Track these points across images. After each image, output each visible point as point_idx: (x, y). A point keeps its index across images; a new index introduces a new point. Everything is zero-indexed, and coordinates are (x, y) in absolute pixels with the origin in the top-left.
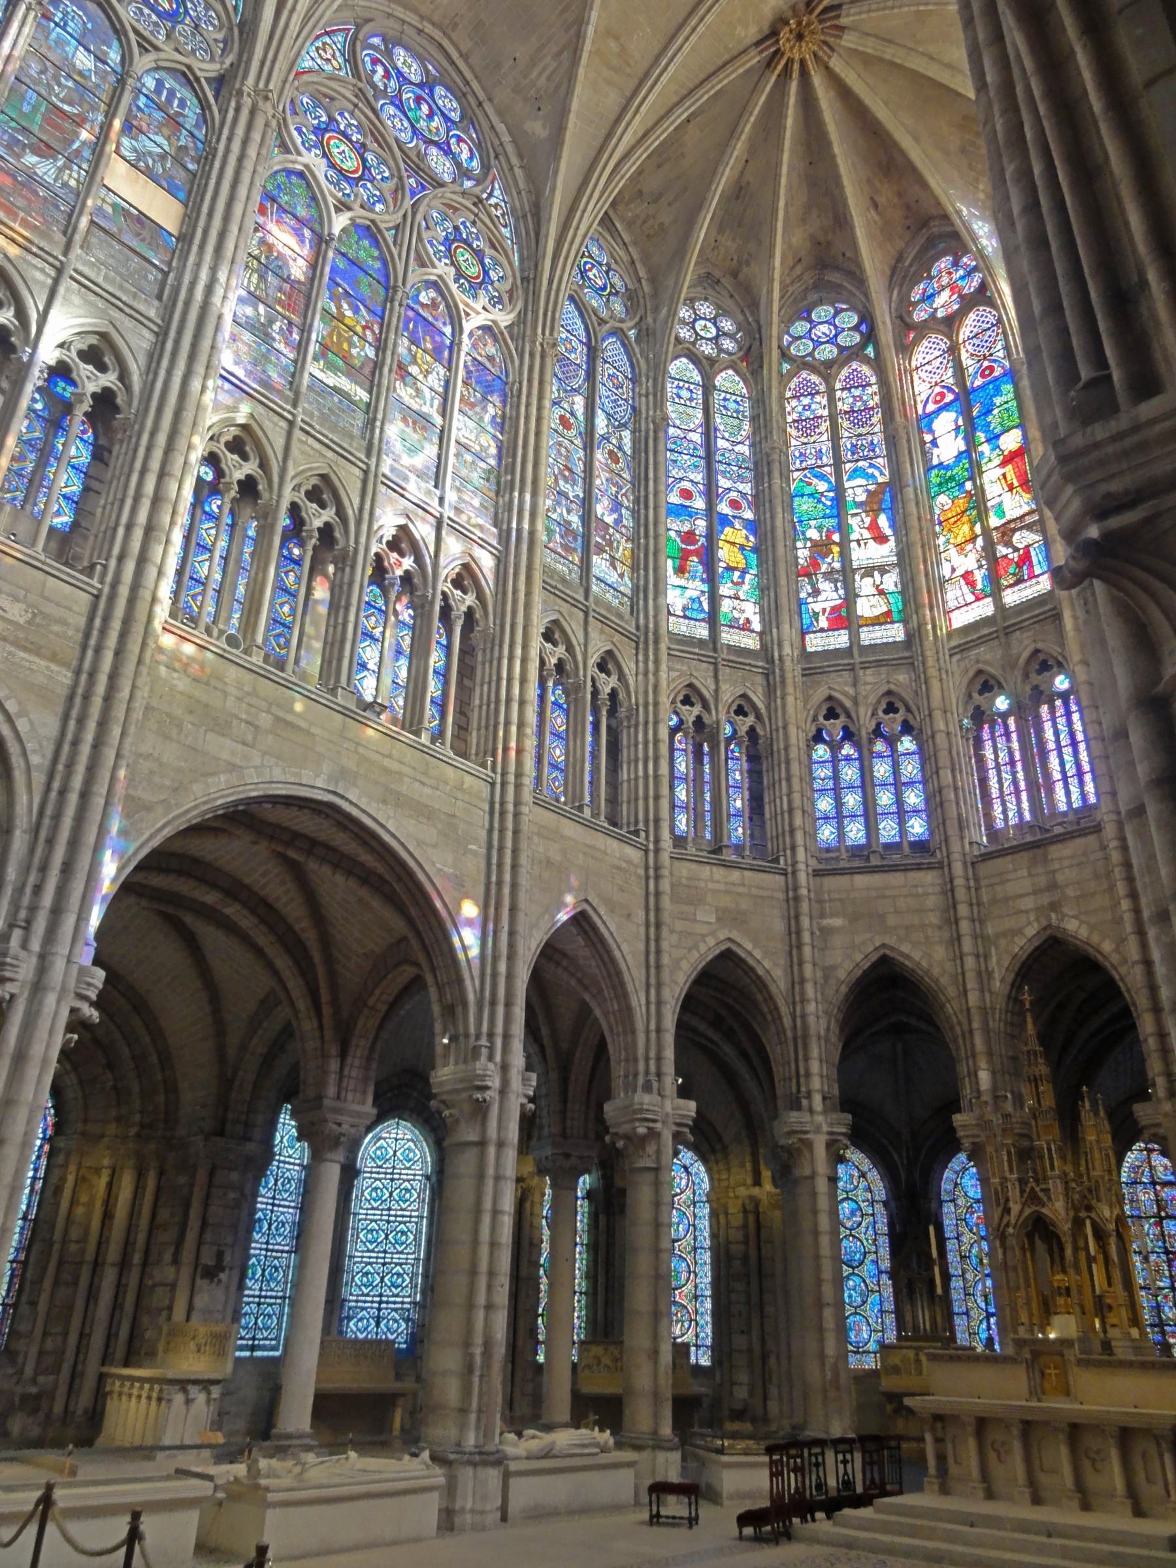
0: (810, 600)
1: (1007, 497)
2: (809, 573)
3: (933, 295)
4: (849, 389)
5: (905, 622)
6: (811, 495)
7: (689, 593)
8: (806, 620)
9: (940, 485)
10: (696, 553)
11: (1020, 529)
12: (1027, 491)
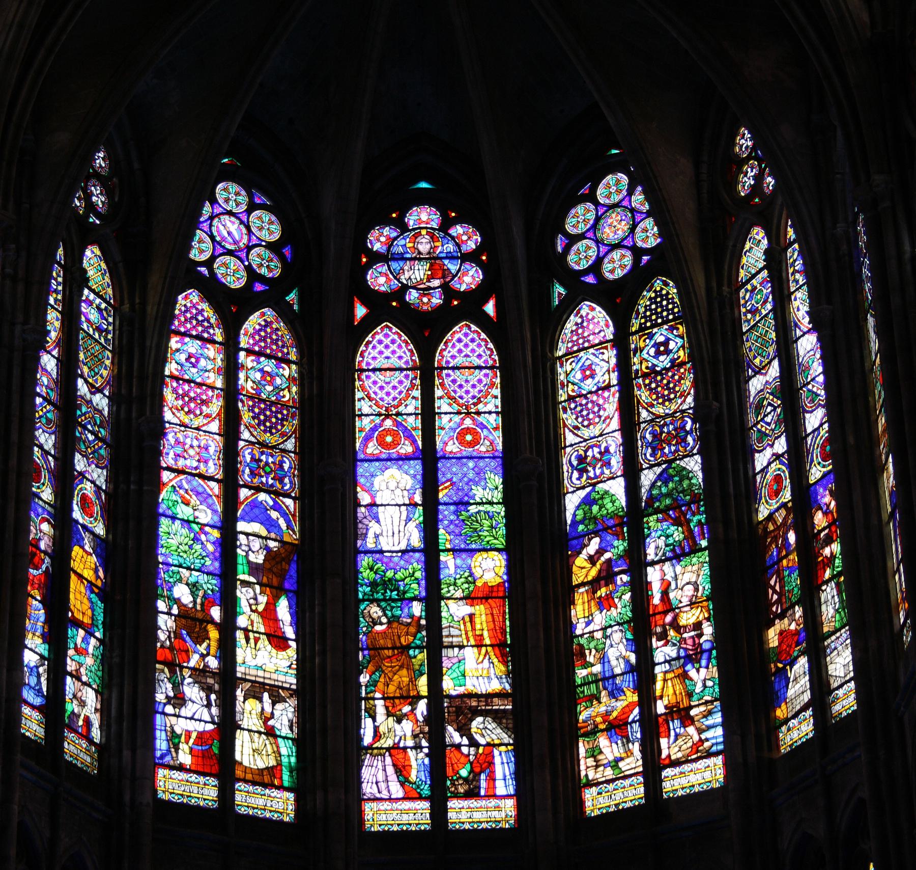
0: (169, 709)
1: (470, 653)
3: (401, 258)
8: (161, 744)
9: (373, 584)
11: (485, 713)
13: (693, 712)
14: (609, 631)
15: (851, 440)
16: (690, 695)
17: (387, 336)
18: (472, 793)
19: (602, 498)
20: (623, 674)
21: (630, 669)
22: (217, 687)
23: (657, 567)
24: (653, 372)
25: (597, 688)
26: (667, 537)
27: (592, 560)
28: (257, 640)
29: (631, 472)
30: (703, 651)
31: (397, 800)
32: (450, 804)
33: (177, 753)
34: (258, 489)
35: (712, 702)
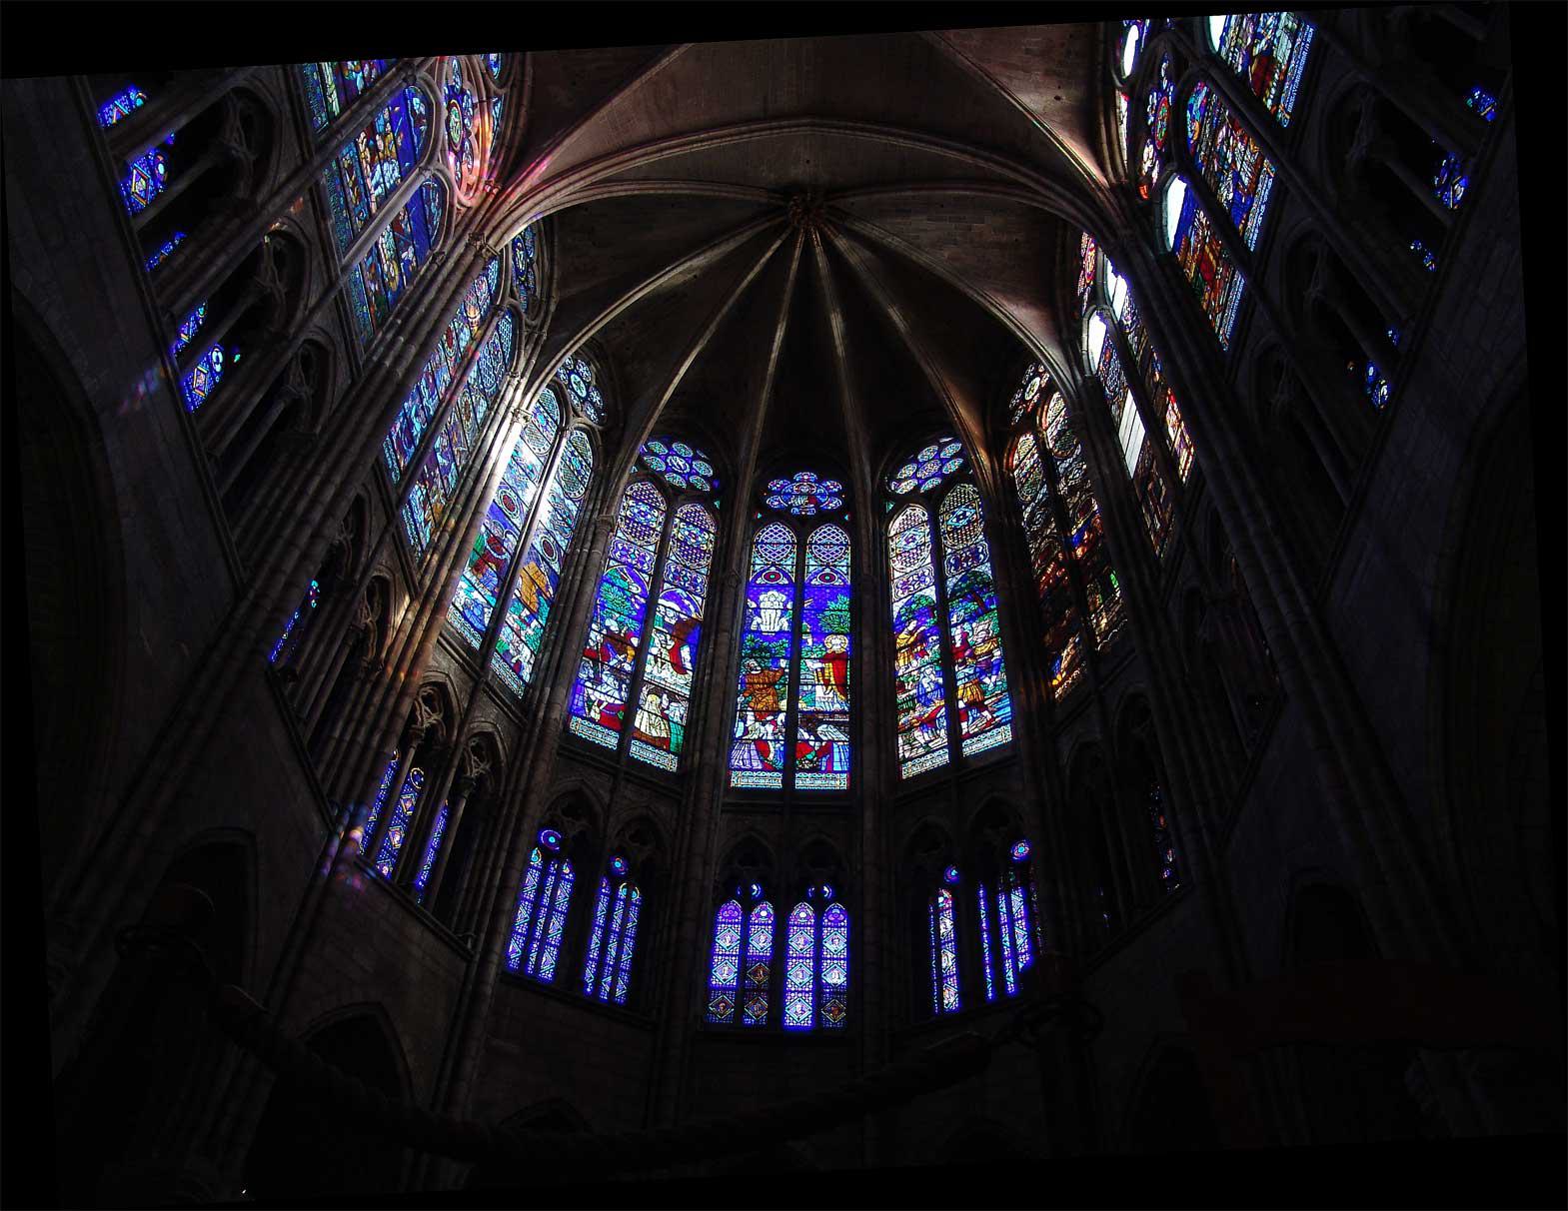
0: (588, 684)
1: (820, 690)
2: (598, 658)
4: (688, 524)
5: (682, 755)
6: (621, 589)
7: (475, 595)
9: (753, 649)
10: (498, 563)
11: (828, 723)
12: (844, 693)
13: (986, 703)
14: (923, 669)
15: (1107, 471)
16: (984, 693)
17: (776, 528)
18: (815, 770)
19: (919, 599)
20: (932, 691)
21: (938, 686)
22: (628, 681)
23: (959, 627)
24: (955, 529)
25: (914, 703)
26: (966, 609)
27: (911, 633)
28: (663, 664)
29: (940, 581)
30: (994, 666)
31: (757, 770)
32: (797, 775)
33: (590, 711)
34: (677, 587)
35: (1001, 694)
